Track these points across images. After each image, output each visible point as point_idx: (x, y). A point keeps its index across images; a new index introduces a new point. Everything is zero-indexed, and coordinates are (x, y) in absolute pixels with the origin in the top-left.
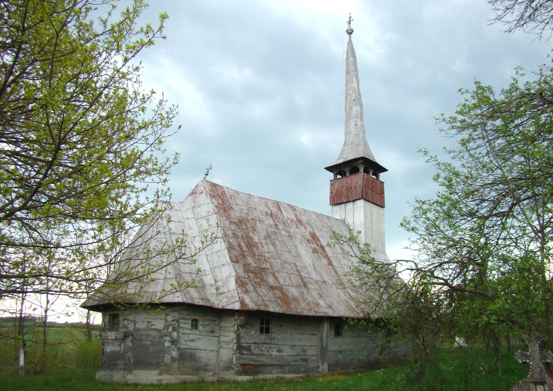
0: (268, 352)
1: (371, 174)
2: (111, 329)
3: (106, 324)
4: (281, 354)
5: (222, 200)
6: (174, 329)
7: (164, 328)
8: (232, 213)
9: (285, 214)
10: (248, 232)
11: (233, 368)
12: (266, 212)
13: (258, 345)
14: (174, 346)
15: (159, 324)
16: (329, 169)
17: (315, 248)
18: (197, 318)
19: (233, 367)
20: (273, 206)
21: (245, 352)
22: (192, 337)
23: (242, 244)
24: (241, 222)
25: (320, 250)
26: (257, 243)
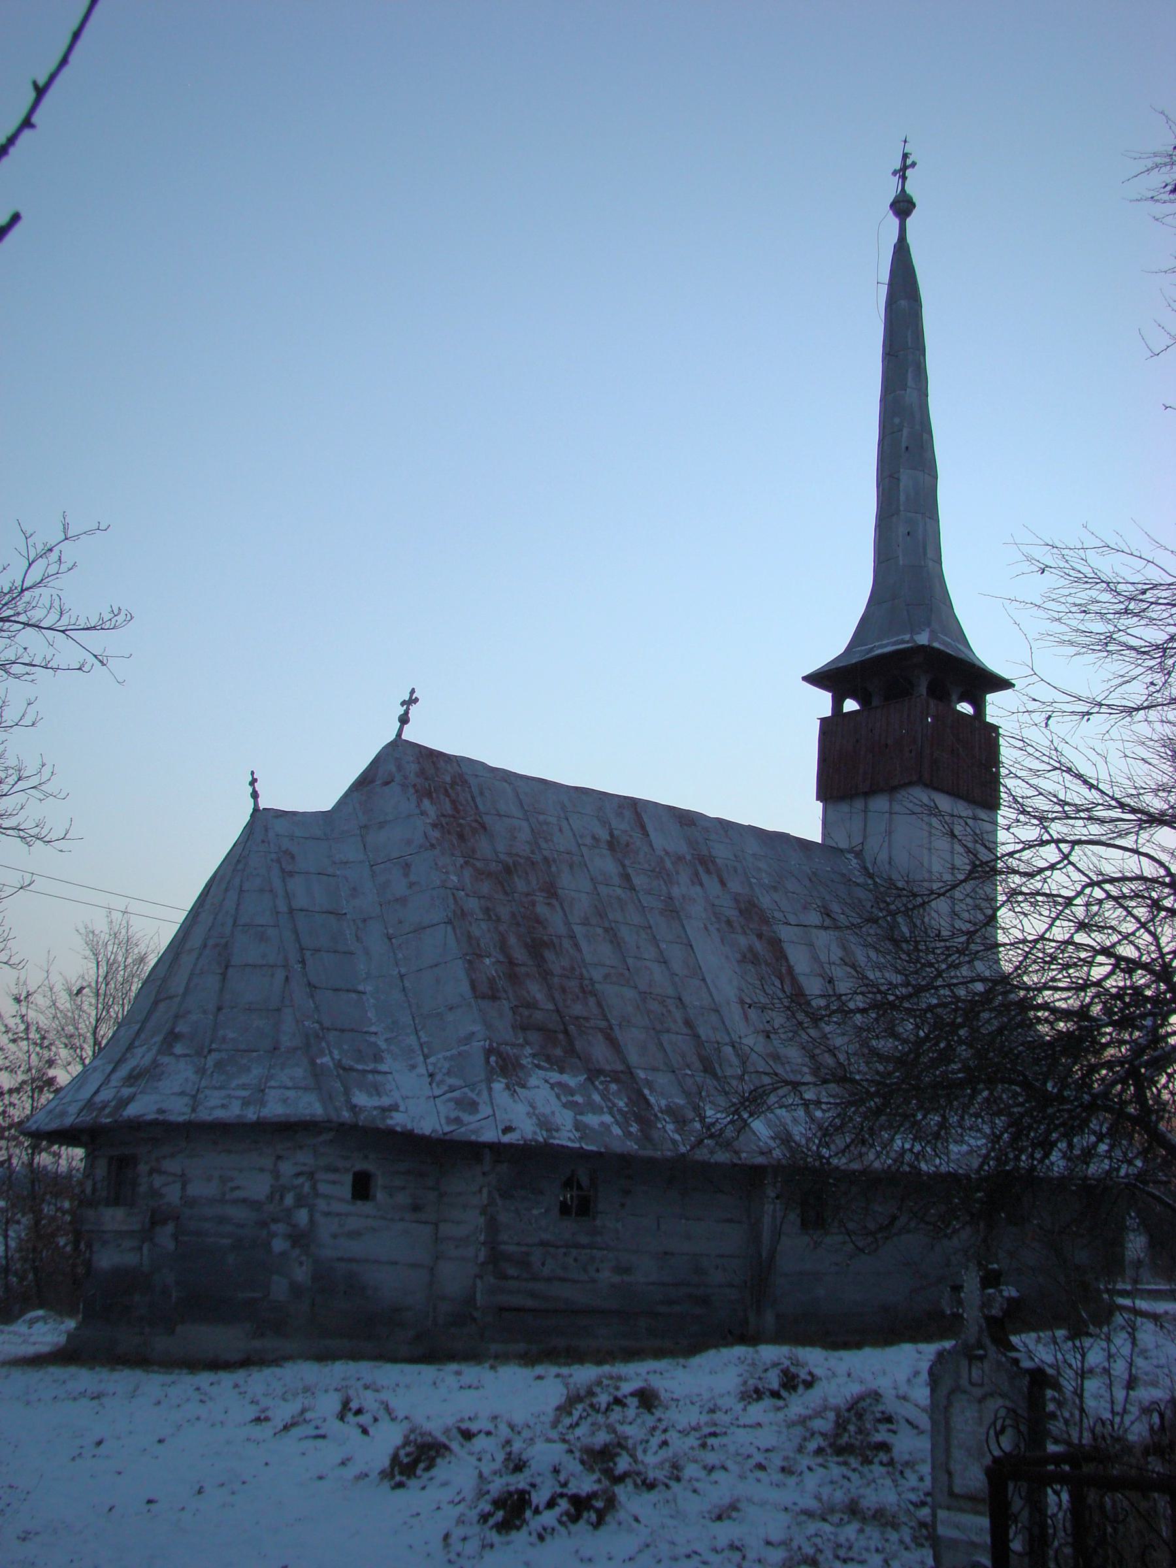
0: (585, 1270)
1: (954, 697)
2: (116, 1200)
3: (99, 1186)
4: (626, 1278)
5: (453, 802)
6: (300, 1201)
7: (270, 1198)
8: (483, 846)
9: (658, 840)
10: (533, 904)
11: (474, 1319)
12: (594, 837)
13: (552, 1250)
14: (297, 1251)
15: (257, 1186)
16: (817, 679)
17: (751, 949)
19: (476, 1314)
20: (620, 815)
21: (512, 1271)
23: (512, 940)
24: (508, 870)
26: (560, 937)
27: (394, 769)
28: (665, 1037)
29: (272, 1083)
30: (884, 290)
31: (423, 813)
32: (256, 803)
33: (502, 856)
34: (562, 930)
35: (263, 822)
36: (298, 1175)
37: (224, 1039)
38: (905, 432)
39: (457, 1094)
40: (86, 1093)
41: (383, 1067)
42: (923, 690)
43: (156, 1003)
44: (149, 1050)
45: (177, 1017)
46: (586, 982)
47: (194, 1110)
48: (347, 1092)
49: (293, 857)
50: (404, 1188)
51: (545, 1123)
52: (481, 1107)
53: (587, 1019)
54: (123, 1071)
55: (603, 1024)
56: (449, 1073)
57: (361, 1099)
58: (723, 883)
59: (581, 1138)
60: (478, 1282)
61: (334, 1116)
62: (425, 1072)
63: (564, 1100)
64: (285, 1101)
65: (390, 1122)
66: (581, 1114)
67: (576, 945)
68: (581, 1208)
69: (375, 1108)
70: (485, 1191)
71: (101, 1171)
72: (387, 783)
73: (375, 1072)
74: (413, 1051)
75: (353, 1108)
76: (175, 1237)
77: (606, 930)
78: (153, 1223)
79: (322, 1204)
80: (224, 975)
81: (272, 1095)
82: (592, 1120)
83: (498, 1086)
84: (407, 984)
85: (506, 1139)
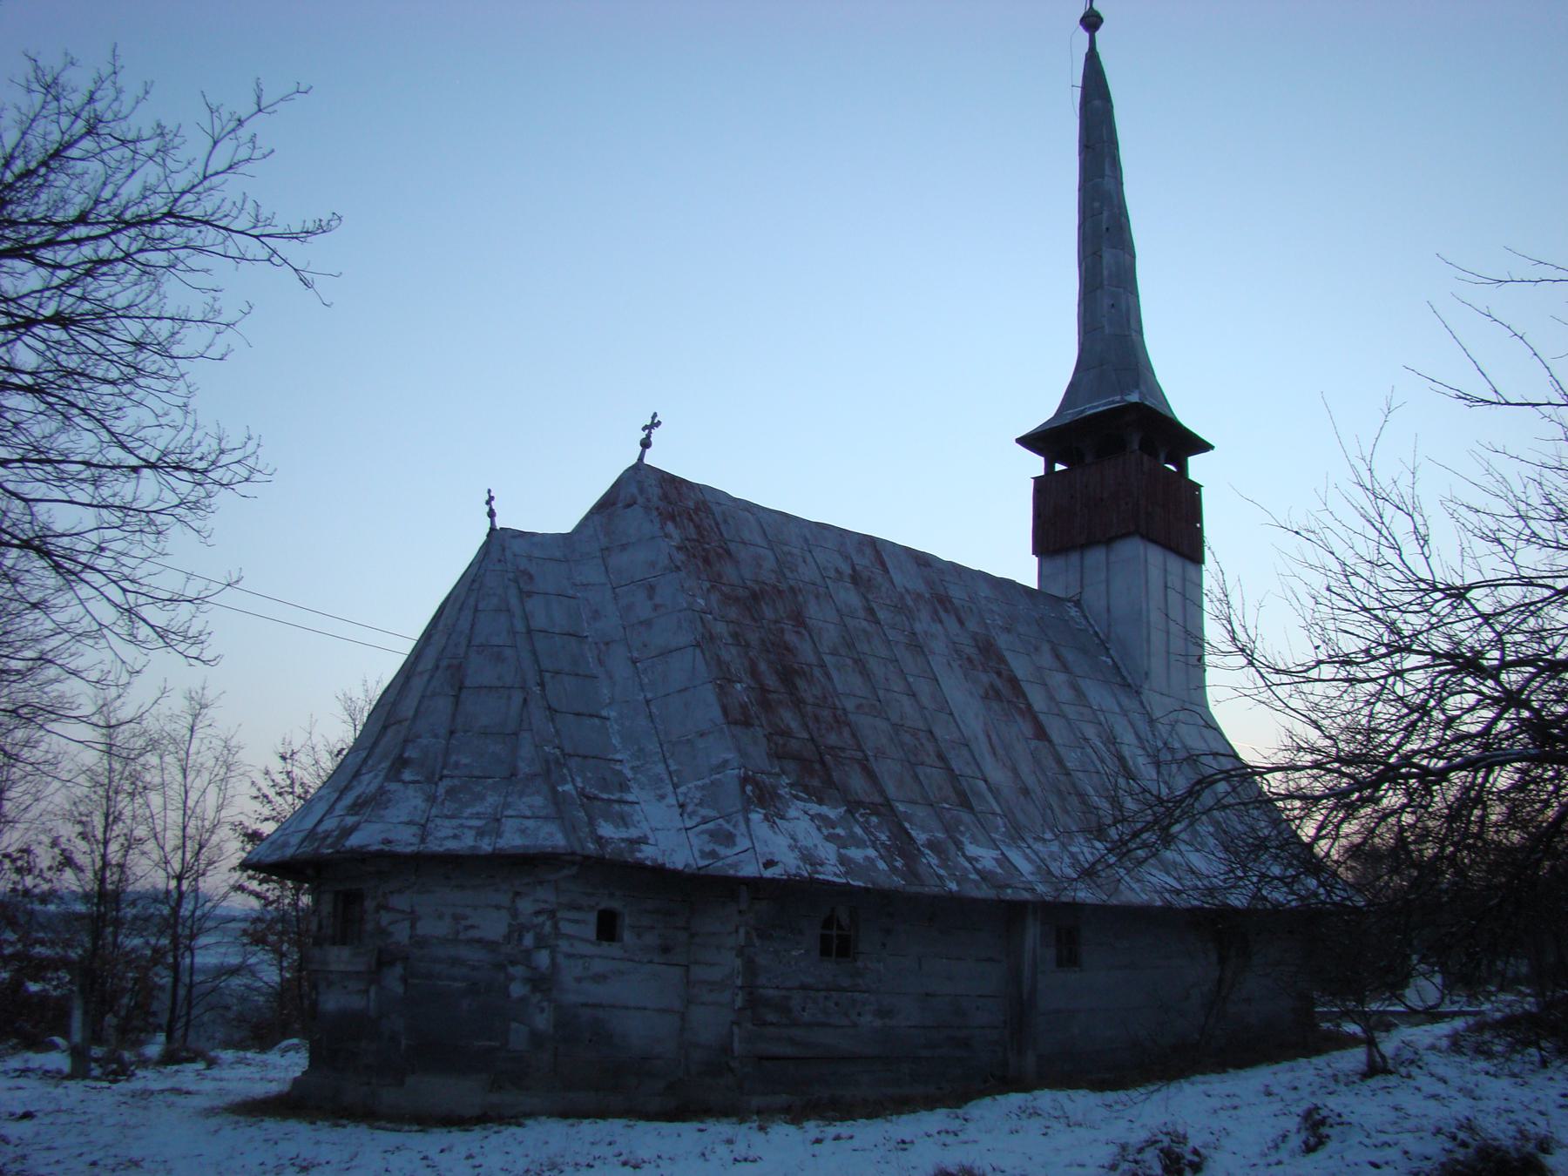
1: (1162, 457)
2: (342, 939)
5: (697, 527)
6: (541, 942)
7: (508, 938)
8: (729, 571)
9: (898, 579)
10: (782, 631)
12: (837, 570)
14: (538, 996)
15: (493, 926)
16: (1030, 441)
17: (992, 685)
18: (616, 905)
19: (732, 1064)
21: (771, 1017)
22: (598, 966)
23: (763, 666)
24: (755, 597)
25: (1006, 692)
27: (635, 491)
28: (920, 770)
29: (510, 812)
30: (1078, 93)
31: (667, 536)
32: (492, 522)
33: (749, 583)
34: (812, 659)
35: (499, 542)
36: (538, 913)
37: (457, 765)
38: (1105, 214)
39: (710, 825)
40: (309, 823)
41: (631, 798)
42: (1136, 446)
43: (385, 728)
44: (376, 776)
45: (406, 741)
46: (839, 712)
47: (423, 841)
48: (591, 822)
49: (531, 577)
50: (653, 928)
51: (808, 857)
52: (738, 839)
53: (843, 749)
54: (348, 800)
55: (859, 755)
56: (701, 804)
57: (607, 830)
58: (961, 622)
59: (847, 873)
60: (736, 1029)
61: (578, 848)
62: (674, 802)
63: (825, 832)
64: (523, 831)
65: (638, 855)
66: (845, 847)
67: (828, 676)
68: (838, 946)
69: (623, 840)
70: (742, 931)
71: (327, 908)
72: (629, 506)
73: (621, 801)
74: (662, 780)
75: (599, 840)
76: (404, 980)
77: (856, 661)
78: (381, 964)
79: (564, 945)
80: (457, 697)
81: (509, 825)
82: (856, 854)
83: (756, 817)
84: (654, 710)
85: (768, 873)
